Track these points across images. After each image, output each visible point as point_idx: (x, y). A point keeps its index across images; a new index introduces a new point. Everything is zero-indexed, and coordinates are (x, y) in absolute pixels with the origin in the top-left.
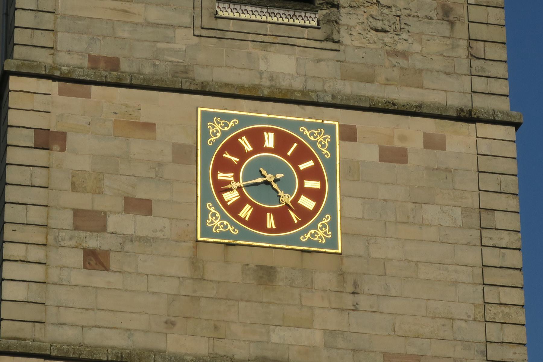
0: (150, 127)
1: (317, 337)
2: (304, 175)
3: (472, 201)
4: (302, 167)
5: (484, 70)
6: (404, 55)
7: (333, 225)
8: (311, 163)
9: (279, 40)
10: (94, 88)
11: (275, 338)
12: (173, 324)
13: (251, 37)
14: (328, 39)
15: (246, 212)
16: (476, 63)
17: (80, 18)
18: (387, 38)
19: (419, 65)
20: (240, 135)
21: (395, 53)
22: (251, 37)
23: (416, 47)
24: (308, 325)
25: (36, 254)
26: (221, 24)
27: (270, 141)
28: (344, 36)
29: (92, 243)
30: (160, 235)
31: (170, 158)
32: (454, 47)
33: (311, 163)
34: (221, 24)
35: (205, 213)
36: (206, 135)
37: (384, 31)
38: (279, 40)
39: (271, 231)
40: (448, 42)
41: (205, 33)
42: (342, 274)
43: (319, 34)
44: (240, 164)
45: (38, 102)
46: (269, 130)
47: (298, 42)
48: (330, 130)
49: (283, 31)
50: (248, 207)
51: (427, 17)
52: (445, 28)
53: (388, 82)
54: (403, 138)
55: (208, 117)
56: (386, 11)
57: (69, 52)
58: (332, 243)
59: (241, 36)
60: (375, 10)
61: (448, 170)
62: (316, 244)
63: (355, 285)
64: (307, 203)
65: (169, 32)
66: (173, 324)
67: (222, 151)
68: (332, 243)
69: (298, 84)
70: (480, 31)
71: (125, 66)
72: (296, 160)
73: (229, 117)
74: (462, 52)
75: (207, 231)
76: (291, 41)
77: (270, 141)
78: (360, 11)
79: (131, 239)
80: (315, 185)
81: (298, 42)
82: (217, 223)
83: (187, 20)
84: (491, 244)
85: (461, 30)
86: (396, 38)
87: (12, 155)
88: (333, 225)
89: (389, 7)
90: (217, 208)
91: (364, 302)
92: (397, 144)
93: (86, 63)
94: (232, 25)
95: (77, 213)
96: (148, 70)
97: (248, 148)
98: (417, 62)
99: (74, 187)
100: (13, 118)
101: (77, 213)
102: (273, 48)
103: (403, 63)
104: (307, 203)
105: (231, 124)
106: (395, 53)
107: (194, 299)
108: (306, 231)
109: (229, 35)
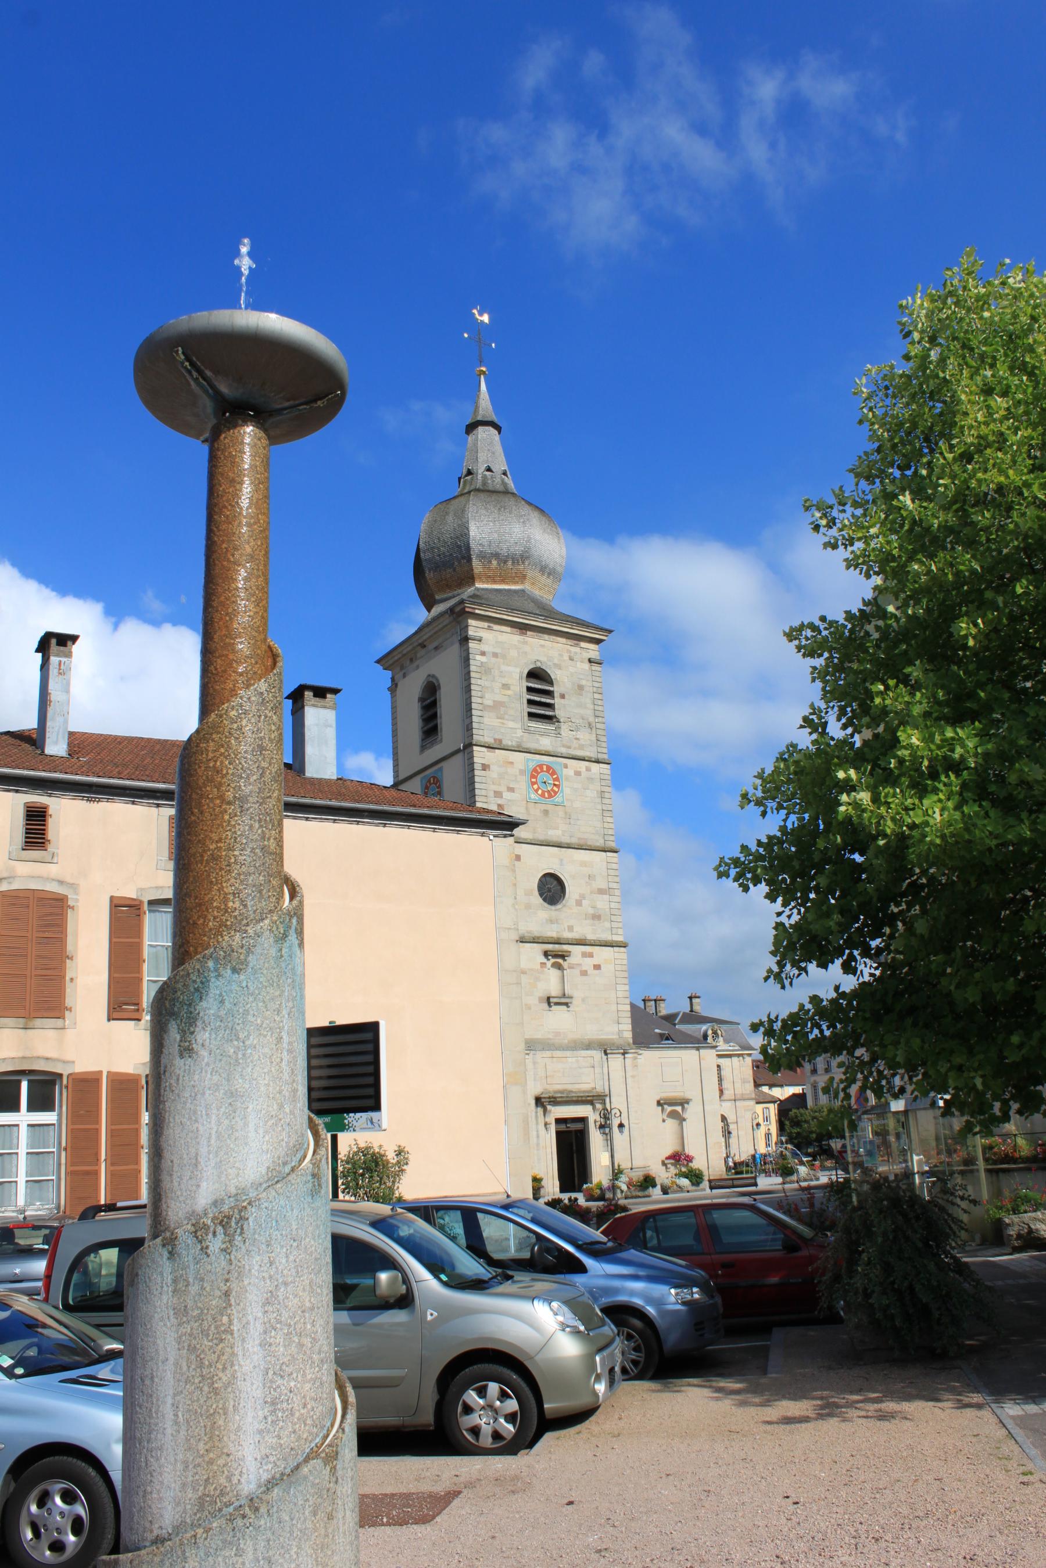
0: (512, 763)
3: (599, 788)
15: (540, 792)
18: (574, 733)
21: (576, 739)
24: (557, 828)
28: (562, 732)
29: (499, 802)
42: (566, 813)
45: (481, 754)
53: (575, 748)
60: (570, 724)
68: (563, 802)
70: (599, 732)
75: (530, 798)
79: (509, 800)
85: (594, 729)
87: (476, 773)
91: (572, 822)
93: (493, 741)
95: (495, 792)
96: (510, 743)
98: (582, 742)
100: (476, 760)
101: (495, 792)
104: (556, 789)
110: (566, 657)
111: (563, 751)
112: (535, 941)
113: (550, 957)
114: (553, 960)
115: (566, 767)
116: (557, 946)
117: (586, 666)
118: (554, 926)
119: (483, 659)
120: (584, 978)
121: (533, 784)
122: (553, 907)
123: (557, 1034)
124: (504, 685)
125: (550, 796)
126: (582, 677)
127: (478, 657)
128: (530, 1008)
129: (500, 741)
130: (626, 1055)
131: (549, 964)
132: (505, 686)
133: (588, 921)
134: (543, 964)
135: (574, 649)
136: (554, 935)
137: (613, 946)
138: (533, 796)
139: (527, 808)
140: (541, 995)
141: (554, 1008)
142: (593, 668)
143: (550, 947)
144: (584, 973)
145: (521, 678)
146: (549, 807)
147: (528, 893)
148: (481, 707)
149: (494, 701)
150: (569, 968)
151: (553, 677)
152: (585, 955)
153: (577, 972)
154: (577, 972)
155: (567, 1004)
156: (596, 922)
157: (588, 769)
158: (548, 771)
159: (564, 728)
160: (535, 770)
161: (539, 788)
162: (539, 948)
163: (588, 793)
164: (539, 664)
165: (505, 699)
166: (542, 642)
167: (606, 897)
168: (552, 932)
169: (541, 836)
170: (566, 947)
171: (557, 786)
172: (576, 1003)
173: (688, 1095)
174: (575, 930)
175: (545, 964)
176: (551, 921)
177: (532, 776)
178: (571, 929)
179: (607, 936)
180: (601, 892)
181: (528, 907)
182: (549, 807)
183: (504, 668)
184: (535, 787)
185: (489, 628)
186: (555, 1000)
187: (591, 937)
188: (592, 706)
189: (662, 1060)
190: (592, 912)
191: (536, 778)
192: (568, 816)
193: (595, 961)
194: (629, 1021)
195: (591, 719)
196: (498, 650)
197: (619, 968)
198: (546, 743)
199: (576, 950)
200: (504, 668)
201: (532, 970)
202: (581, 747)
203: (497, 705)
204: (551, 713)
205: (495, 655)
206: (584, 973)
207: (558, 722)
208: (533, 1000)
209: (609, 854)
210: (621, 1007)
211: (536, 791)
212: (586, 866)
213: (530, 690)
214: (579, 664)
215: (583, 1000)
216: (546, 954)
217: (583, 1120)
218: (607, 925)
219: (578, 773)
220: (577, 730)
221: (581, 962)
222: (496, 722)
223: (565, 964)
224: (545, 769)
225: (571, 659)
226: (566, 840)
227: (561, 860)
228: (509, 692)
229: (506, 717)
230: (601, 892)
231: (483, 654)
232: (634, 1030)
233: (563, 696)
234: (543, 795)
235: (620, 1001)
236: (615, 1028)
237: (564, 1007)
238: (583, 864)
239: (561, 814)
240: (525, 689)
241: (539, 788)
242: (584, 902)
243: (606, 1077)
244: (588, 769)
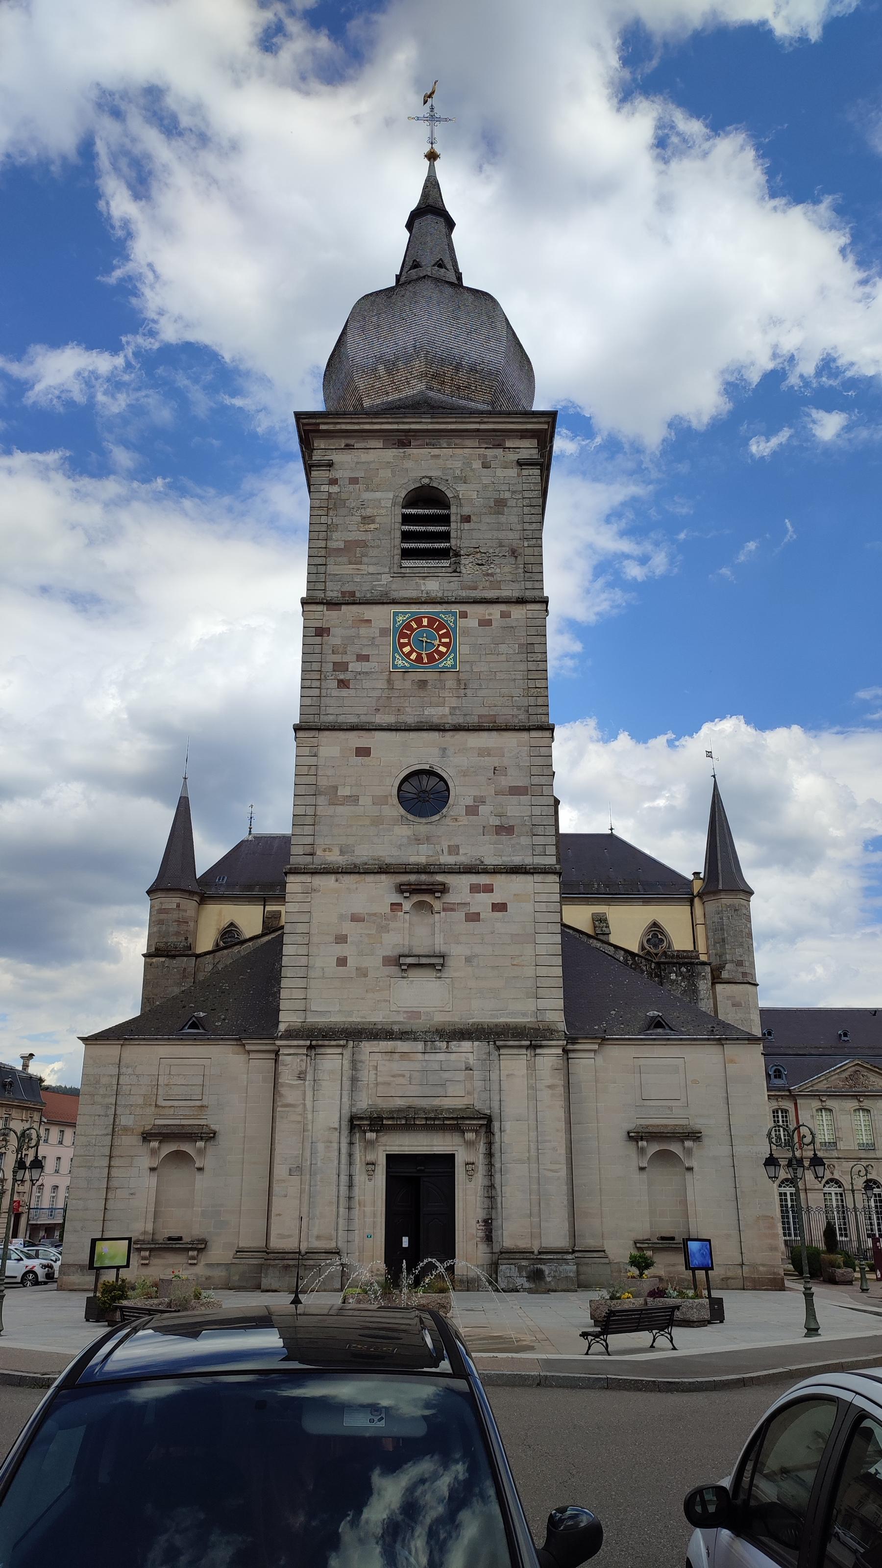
0: (369, 621)
1: (447, 711)
2: (441, 636)
3: (523, 641)
4: (440, 633)
5: (531, 578)
6: (492, 575)
7: (455, 658)
8: (445, 631)
9: (431, 575)
10: (343, 607)
11: (426, 713)
12: (379, 710)
13: (417, 575)
14: (455, 571)
15: (414, 656)
16: (527, 575)
17: (337, 575)
19: (499, 579)
20: (411, 621)
21: (488, 575)
22: (417, 575)
23: (498, 570)
25: (317, 684)
26: (403, 570)
27: (425, 622)
29: (342, 677)
30: (373, 670)
31: (378, 635)
32: (517, 568)
33: (445, 631)
34: (403, 570)
35: (394, 658)
36: (395, 622)
37: (482, 565)
38: (431, 575)
39: (425, 664)
40: (514, 566)
41: (395, 575)
42: (459, 680)
43: (450, 570)
44: (411, 634)
46: (425, 617)
47: (440, 575)
48: (454, 614)
49: (432, 570)
50: (414, 653)
51: (503, 556)
52: (512, 560)
54: (490, 614)
55: (396, 614)
56: (483, 555)
57: (332, 591)
58: (454, 666)
59: (413, 575)
60: (478, 556)
61: (512, 627)
62: (447, 667)
63: (465, 685)
64: (443, 649)
65: (379, 577)
66: (379, 710)
67: (402, 629)
68: (454, 666)
69: (440, 595)
71: (358, 595)
72: (437, 630)
73: (405, 613)
74: (521, 571)
75: (395, 666)
76: (436, 574)
77: (425, 622)
78: (470, 557)
81: (440, 575)
82: (400, 662)
83: (387, 570)
84: (532, 659)
85: (520, 560)
86: (488, 567)
88: (455, 658)
89: (485, 553)
90: (400, 656)
92: (487, 617)
94: (408, 570)
97: (415, 626)
99: (333, 653)
102: (428, 579)
103: (491, 579)
104: (443, 649)
105: (407, 616)
106: (488, 575)
107: (389, 698)
108: (442, 662)
109: (407, 575)
110: (477, 465)
111: (464, 594)
112: (384, 869)
113: (407, 895)
114: (416, 898)
115: (464, 615)
116: (423, 877)
117: (513, 472)
118: (423, 848)
119: (334, 489)
120: (472, 924)
121: (403, 645)
122: (424, 820)
123: (416, 1014)
124: (364, 518)
126: (503, 488)
127: (325, 488)
128: (366, 975)
129: (353, 594)
130: (538, 1051)
131: (407, 906)
132: (367, 520)
133: (487, 838)
134: (396, 906)
135: (490, 453)
136: (423, 860)
137: (532, 873)
138: (400, 662)
139: (389, 681)
140: (389, 953)
141: (413, 973)
142: (525, 472)
143: (413, 878)
144: (473, 917)
145: (394, 504)
146: (430, 677)
147: (380, 801)
148: (323, 553)
149: (345, 541)
150: (444, 910)
151: (450, 495)
152: (475, 889)
153: (460, 915)
154: (460, 915)
155: (432, 966)
156: (504, 838)
157: (505, 615)
159: (467, 566)
160: (408, 626)
161: (410, 653)
162: (386, 882)
163: (503, 648)
164: (427, 481)
165: (369, 536)
166: (436, 452)
167: (524, 799)
168: (419, 856)
169: (410, 719)
170: (440, 878)
172: (456, 968)
173: (697, 1123)
174: (461, 851)
175: (401, 904)
176: (417, 840)
178: (454, 850)
179: (517, 860)
180: (515, 791)
181: (377, 821)
182: (430, 677)
183: (366, 496)
184: (407, 649)
185: (348, 447)
186: (409, 960)
187: (491, 860)
188: (519, 527)
189: (642, 1062)
190: (498, 823)
192: (462, 685)
193: (497, 897)
194: (560, 993)
195: (515, 544)
196: (360, 474)
197: (543, 907)
198: (433, 587)
199: (460, 884)
200: (366, 496)
201: (375, 914)
202: (496, 585)
203: (350, 547)
204: (442, 545)
205: (354, 481)
206: (473, 917)
207: (457, 555)
208: (373, 963)
209: (534, 734)
210: (542, 971)
211: (408, 655)
212: (489, 755)
214: (500, 472)
215: (468, 960)
216: (401, 889)
217: (449, 1159)
218: (525, 840)
219: (485, 623)
220: (489, 562)
221: (468, 900)
222: (348, 569)
223: (437, 905)
225: (486, 466)
226: (451, 720)
227: (444, 750)
228: (372, 526)
229: (365, 559)
230: (515, 791)
231: (333, 482)
232: (567, 1010)
233: (467, 519)
234: (419, 659)
235: (541, 960)
236: (530, 1005)
237: (430, 974)
238: (484, 752)
239: (450, 683)
240: (399, 519)
242: (482, 809)
243: (495, 1087)
244: (505, 615)
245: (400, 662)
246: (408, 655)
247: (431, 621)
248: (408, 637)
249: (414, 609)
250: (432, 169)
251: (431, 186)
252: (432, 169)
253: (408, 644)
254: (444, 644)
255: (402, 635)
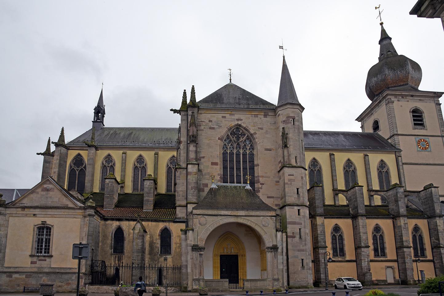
15: (421, 148)
27: (422, 140)
80: (428, 145)
121: (419, 146)
125: (425, 149)
138: (419, 149)
158: (424, 141)
160: (419, 141)
161: (421, 147)
171: (428, 146)
177: (418, 143)
184: (420, 146)
191: (419, 143)
211: (420, 148)
213: (414, 116)
224: (422, 140)
234: (423, 149)
241: (421, 147)
245: (419, 149)
246: (420, 148)
247: (424, 140)
248: (419, 143)
249: (420, 137)
250: (382, 27)
251: (383, 32)
252: (382, 27)
253: (420, 145)
254: (428, 146)
255: (418, 143)
